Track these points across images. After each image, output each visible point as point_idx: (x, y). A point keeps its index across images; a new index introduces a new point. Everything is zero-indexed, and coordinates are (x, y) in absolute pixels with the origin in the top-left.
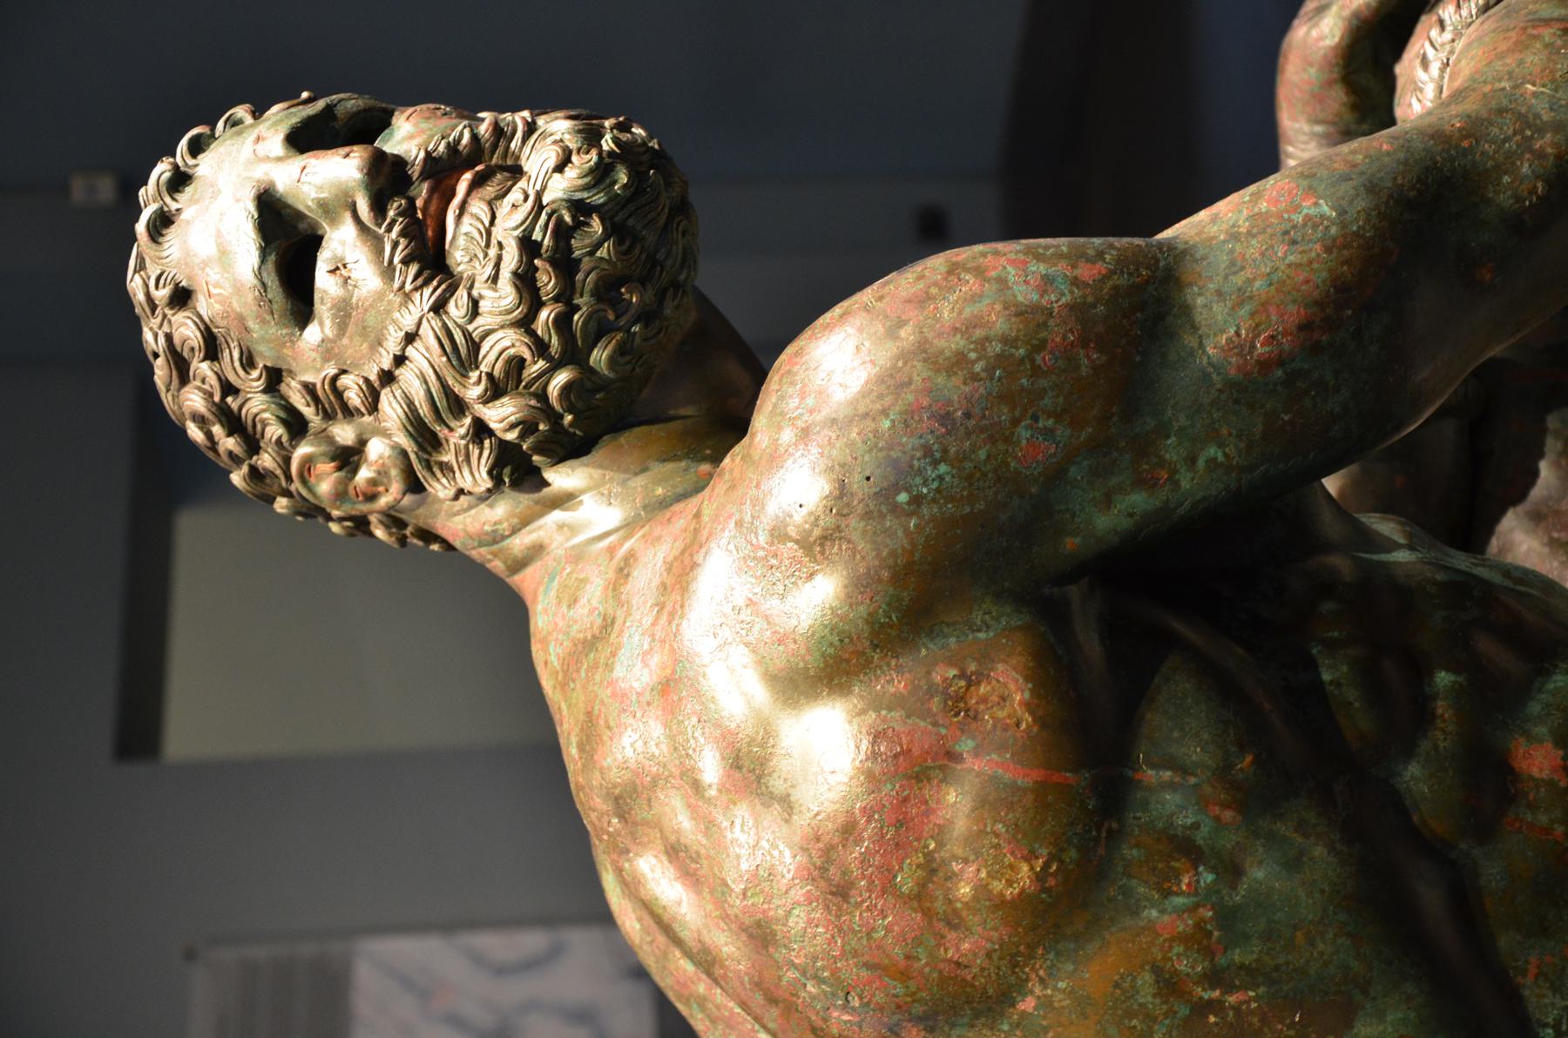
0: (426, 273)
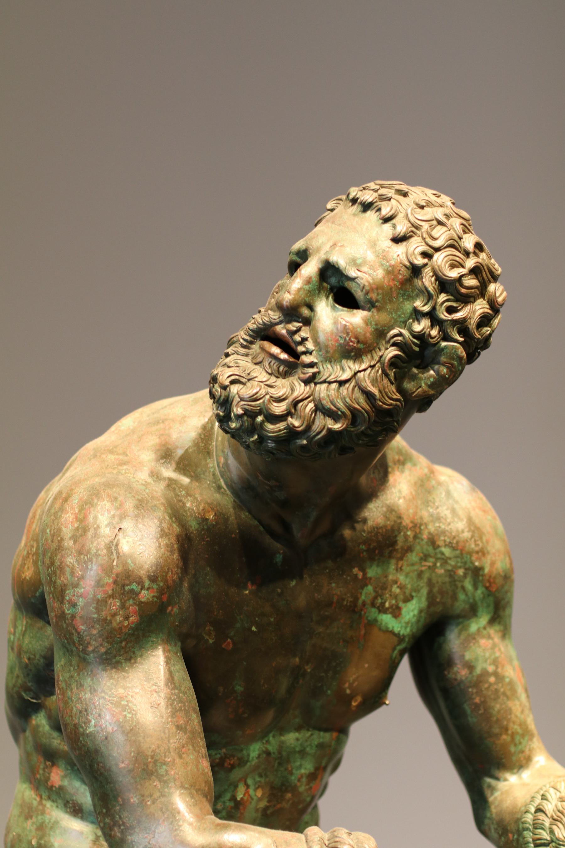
0: (251, 332)
